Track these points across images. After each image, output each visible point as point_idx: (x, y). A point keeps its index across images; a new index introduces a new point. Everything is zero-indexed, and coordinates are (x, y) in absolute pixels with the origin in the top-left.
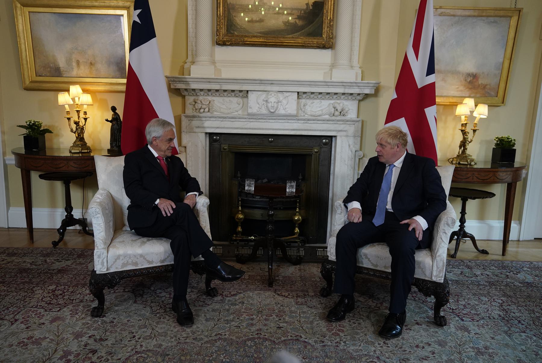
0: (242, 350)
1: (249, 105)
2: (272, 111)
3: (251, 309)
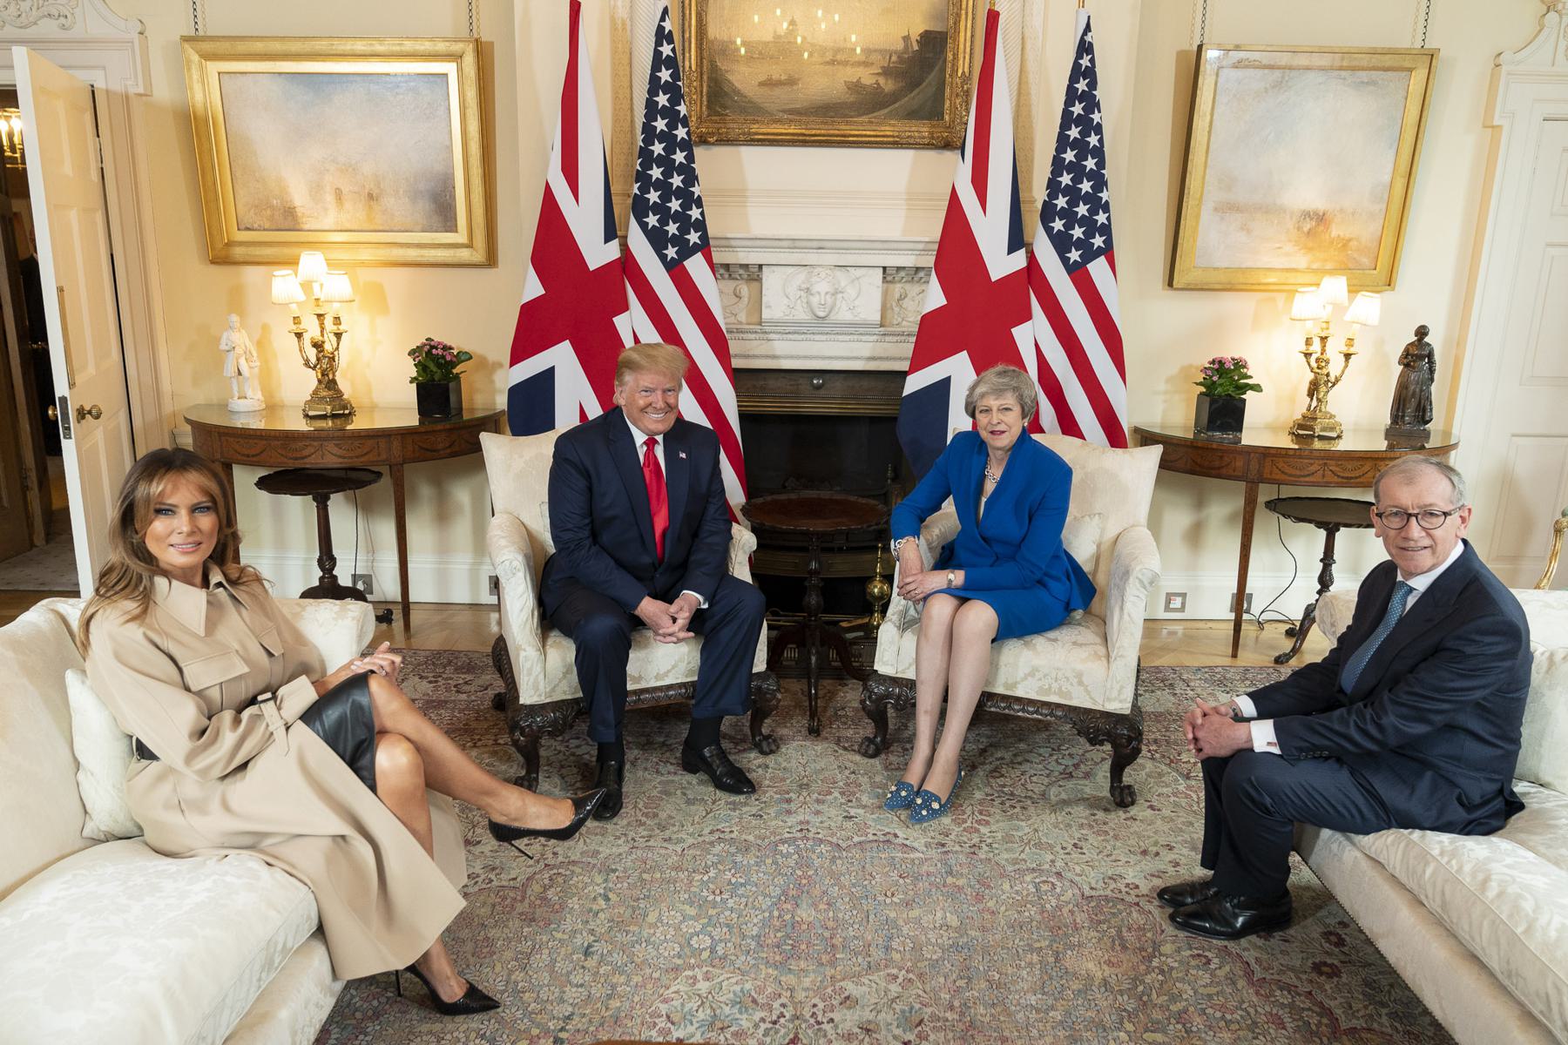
0: (769, 861)
1: (764, 299)
2: (822, 314)
3: (783, 780)
